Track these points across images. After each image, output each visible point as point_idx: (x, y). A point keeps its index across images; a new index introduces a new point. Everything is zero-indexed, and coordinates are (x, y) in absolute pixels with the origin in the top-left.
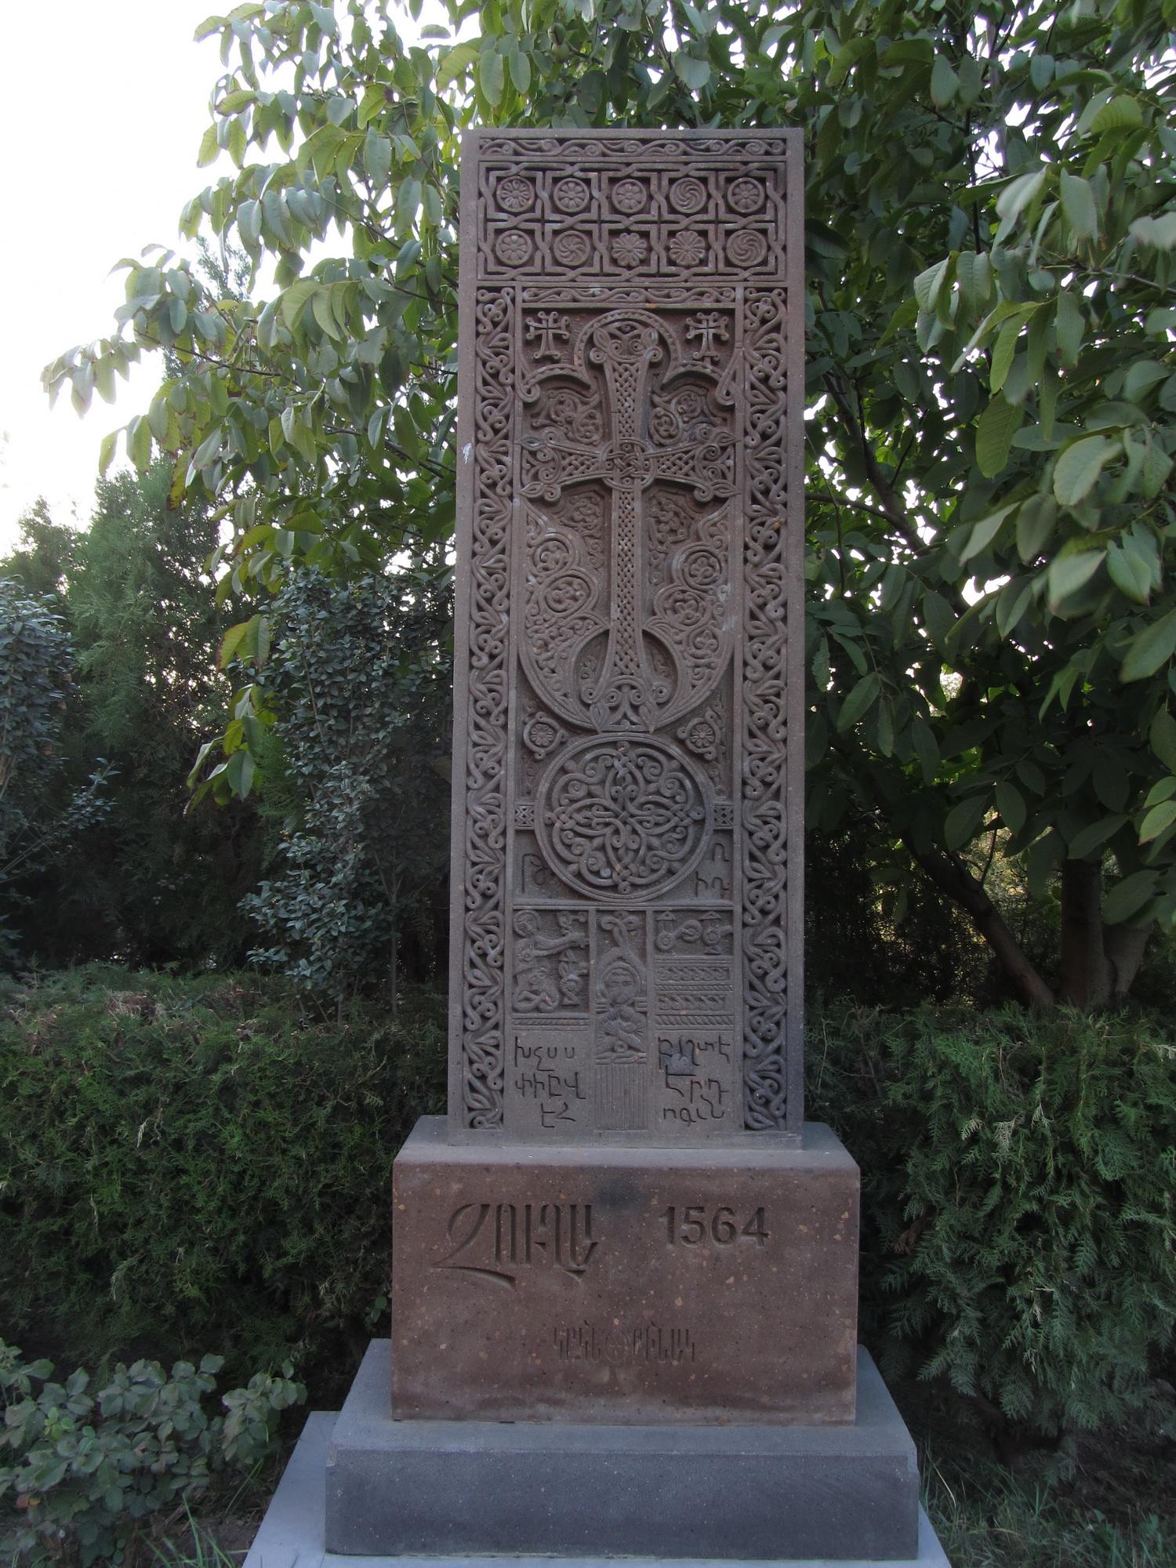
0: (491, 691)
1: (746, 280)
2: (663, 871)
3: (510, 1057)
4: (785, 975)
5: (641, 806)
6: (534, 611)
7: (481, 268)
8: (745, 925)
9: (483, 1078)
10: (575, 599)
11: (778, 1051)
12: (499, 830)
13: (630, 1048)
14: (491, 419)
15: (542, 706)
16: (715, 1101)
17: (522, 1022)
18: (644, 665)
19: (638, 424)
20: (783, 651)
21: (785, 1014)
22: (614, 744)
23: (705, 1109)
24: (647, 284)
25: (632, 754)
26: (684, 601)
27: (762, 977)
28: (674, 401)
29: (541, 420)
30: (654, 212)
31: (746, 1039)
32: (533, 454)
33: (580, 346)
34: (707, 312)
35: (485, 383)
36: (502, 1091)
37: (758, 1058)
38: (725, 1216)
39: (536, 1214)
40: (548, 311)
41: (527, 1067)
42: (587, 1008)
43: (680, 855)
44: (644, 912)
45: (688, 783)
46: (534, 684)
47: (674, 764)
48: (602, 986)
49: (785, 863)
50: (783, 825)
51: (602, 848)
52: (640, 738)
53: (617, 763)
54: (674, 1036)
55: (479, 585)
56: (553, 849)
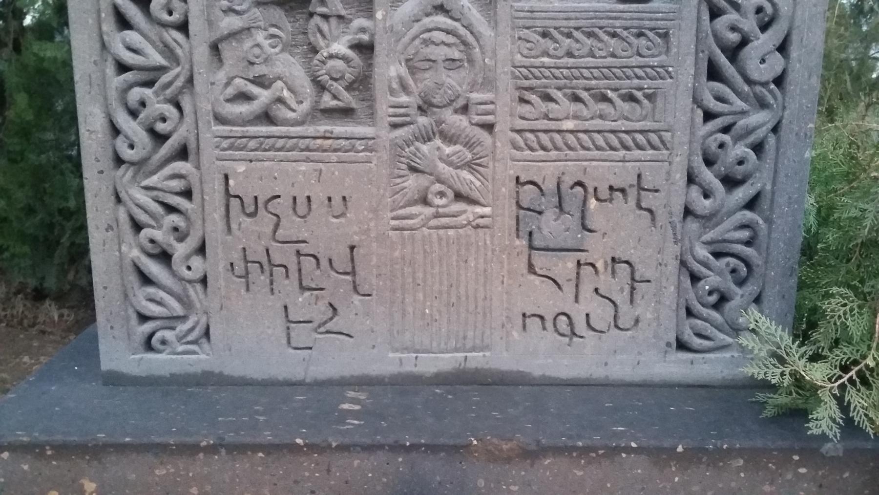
3: (217, 215)
4: (783, 48)
9: (164, 257)
11: (751, 204)
13: (459, 196)
16: (621, 299)
17: (235, 144)
21: (775, 130)
23: (601, 313)
27: (734, 53)
31: (691, 179)
36: (204, 281)
37: (709, 219)
41: (252, 233)
42: (372, 116)
48: (403, 70)
54: (547, 171)
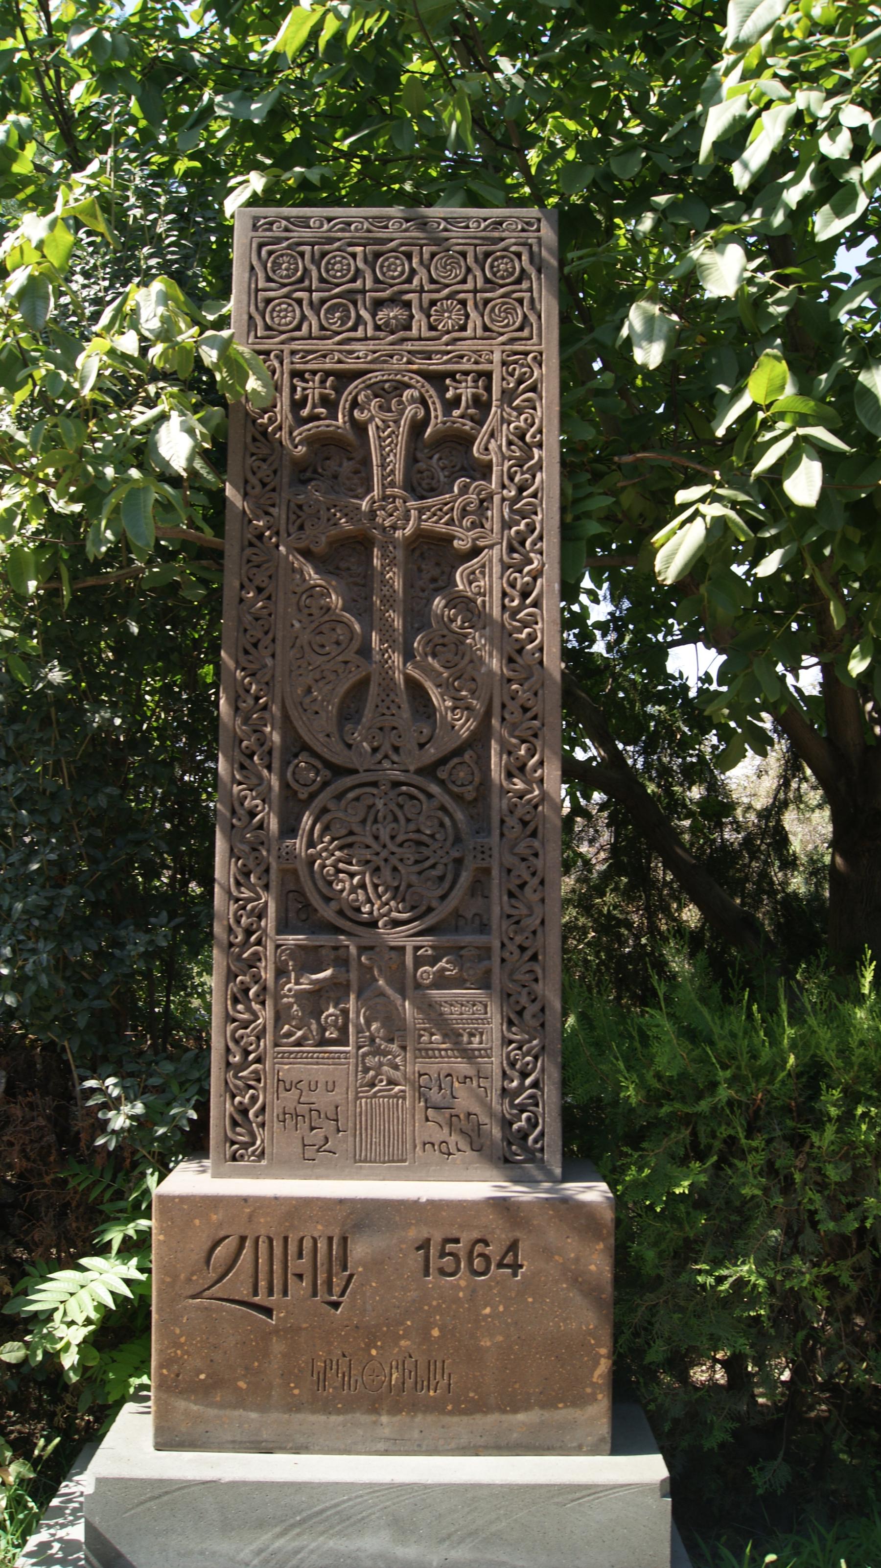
0: (255, 731)
1: (503, 344)
2: (423, 908)
4: (543, 1010)
5: (401, 845)
7: (252, 334)
8: (503, 960)
10: (338, 643)
11: (535, 1085)
12: (263, 867)
14: (260, 474)
15: (305, 747)
18: (405, 706)
19: (399, 477)
20: (540, 692)
21: (543, 1048)
22: (375, 784)
24: (409, 348)
25: (392, 794)
26: (444, 645)
27: (520, 1013)
28: (436, 456)
29: (308, 474)
30: (416, 281)
32: (300, 507)
33: (344, 403)
34: (466, 373)
35: (254, 440)
38: (479, 1248)
39: (292, 1248)
40: (314, 373)
43: (440, 892)
44: (403, 949)
45: (447, 821)
46: (298, 724)
47: (435, 803)
49: (543, 900)
50: (538, 863)
51: (363, 886)
52: (402, 777)
53: (377, 801)
55: (246, 630)
56: (315, 884)
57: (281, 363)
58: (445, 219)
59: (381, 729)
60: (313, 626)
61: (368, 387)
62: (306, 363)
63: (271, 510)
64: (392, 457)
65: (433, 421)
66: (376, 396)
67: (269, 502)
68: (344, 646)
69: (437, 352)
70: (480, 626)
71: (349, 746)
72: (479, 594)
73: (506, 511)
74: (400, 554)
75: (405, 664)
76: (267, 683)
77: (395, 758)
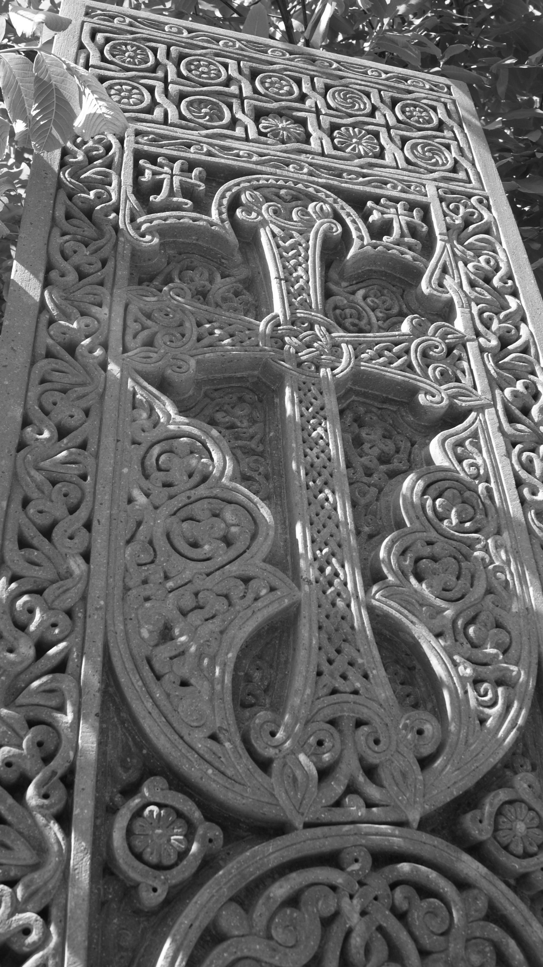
0: (31, 723)
6: (145, 558)
18: (378, 673)
19: (315, 296)
22: (332, 859)
25: (378, 883)
26: (434, 559)
28: (361, 293)
52: (396, 839)
55: (26, 503)
57: (121, 141)
58: (338, 62)
59: (333, 722)
60: (175, 504)
61: (257, 188)
62: (162, 146)
63: (95, 310)
64: (301, 271)
65: (356, 242)
66: (267, 200)
67: (91, 298)
68: (239, 546)
69: (350, 173)
70: (492, 528)
71: (265, 765)
72: (477, 476)
73: (491, 365)
74: (332, 404)
75: (367, 588)
76: (69, 613)
77: (373, 792)
